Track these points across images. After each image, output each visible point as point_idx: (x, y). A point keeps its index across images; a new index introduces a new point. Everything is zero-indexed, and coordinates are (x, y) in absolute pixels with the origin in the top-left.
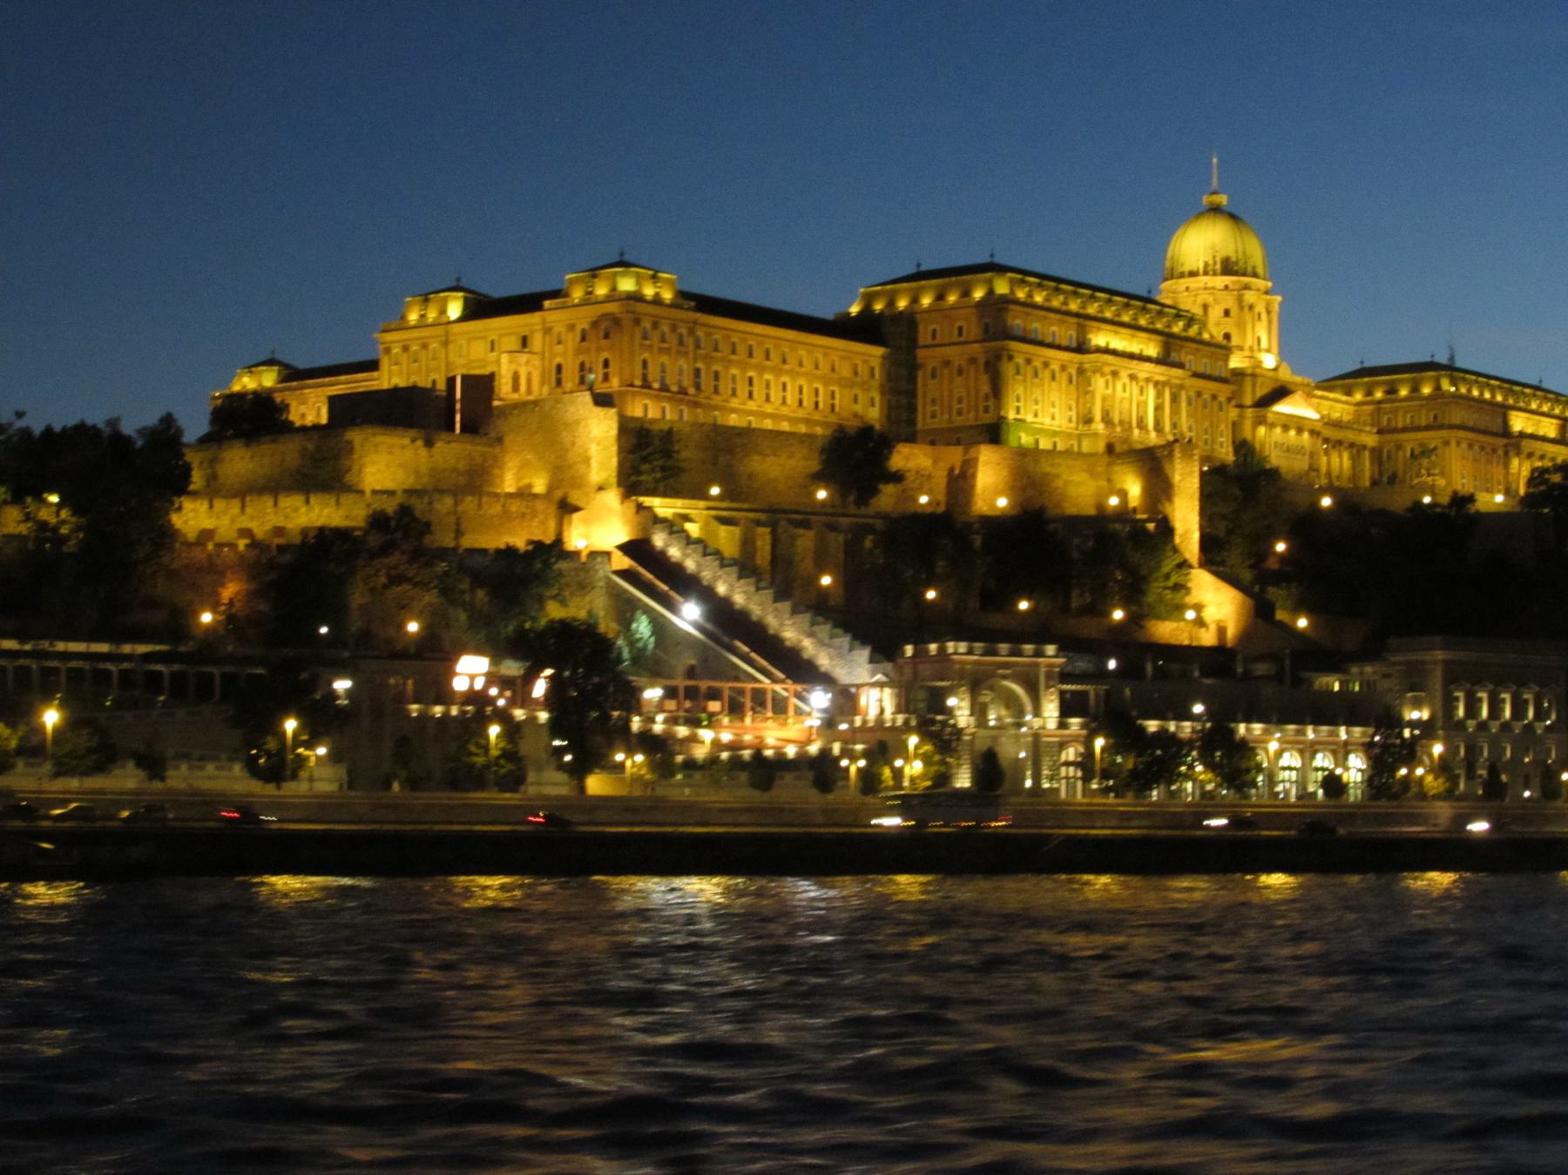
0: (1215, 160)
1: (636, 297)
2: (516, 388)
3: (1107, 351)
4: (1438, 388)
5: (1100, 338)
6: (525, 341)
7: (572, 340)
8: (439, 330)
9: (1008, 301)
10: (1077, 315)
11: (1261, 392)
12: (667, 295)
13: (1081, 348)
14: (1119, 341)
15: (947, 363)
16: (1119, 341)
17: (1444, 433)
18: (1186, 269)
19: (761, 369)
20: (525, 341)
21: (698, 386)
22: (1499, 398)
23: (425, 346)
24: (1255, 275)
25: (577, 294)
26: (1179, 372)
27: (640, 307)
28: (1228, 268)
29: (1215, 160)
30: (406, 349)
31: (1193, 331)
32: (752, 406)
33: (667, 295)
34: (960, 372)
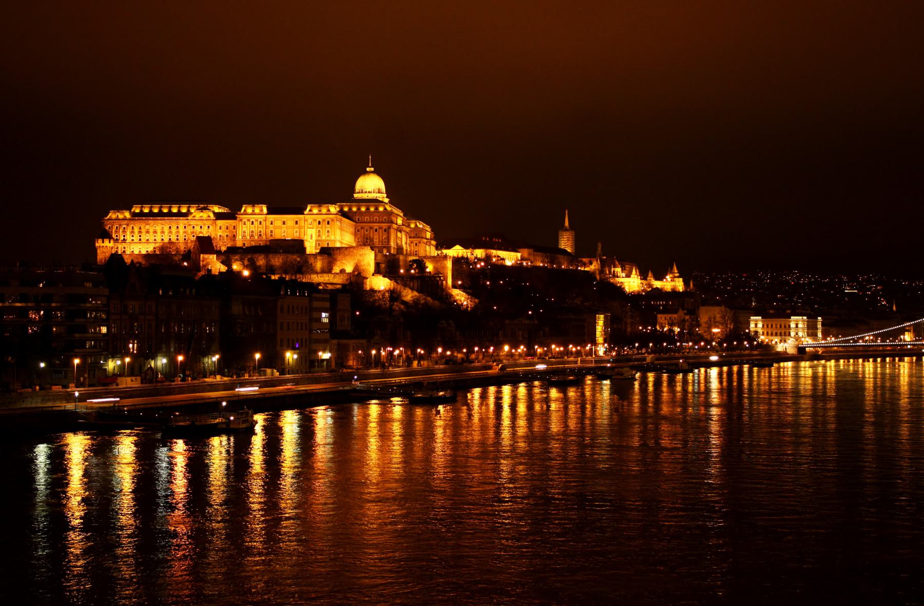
6: (297, 222)
7: (316, 223)
20: (297, 222)
28: (379, 192)
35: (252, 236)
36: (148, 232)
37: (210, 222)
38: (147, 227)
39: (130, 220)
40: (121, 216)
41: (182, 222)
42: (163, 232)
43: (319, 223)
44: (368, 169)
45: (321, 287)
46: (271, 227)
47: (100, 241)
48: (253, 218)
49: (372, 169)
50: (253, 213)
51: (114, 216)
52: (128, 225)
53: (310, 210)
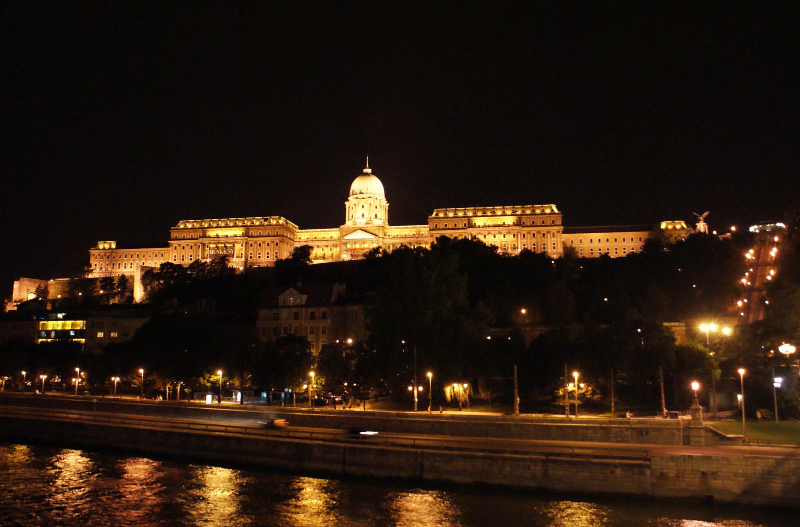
0: (367, 158)
3: (218, 236)
5: (212, 233)
10: (204, 228)
11: (344, 234)
12: (107, 246)
13: (204, 236)
14: (221, 232)
16: (221, 232)
19: (134, 260)
21: (113, 268)
22: (470, 214)
24: (361, 193)
28: (353, 194)
29: (367, 158)
31: (266, 223)
32: (131, 270)
44: (365, 170)
49: (369, 171)
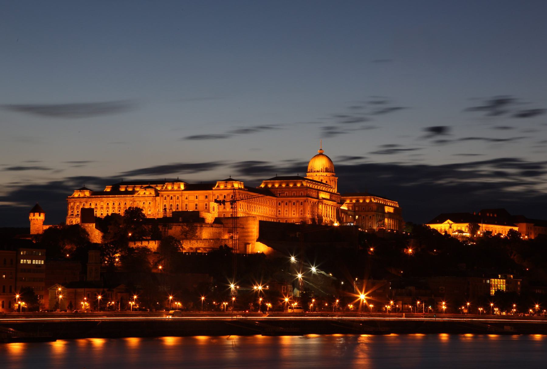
1: (239, 189)
2: (214, 210)
4: (371, 201)
6: (206, 197)
8: (180, 192)
9: (307, 188)
15: (290, 202)
17: (373, 213)
18: (316, 170)
23: (175, 196)
25: (222, 187)
26: (335, 203)
27: (241, 191)
30: (168, 196)
33: (243, 187)
34: (294, 204)
35: (171, 209)
36: (102, 208)
37: (151, 198)
38: (102, 203)
39: (88, 197)
40: (82, 195)
41: (129, 198)
42: (114, 208)
43: (225, 196)
45: (198, 251)
46: (186, 202)
47: (32, 214)
48: (171, 194)
50: (173, 190)
51: (76, 196)
52: (86, 202)
53: (218, 186)
